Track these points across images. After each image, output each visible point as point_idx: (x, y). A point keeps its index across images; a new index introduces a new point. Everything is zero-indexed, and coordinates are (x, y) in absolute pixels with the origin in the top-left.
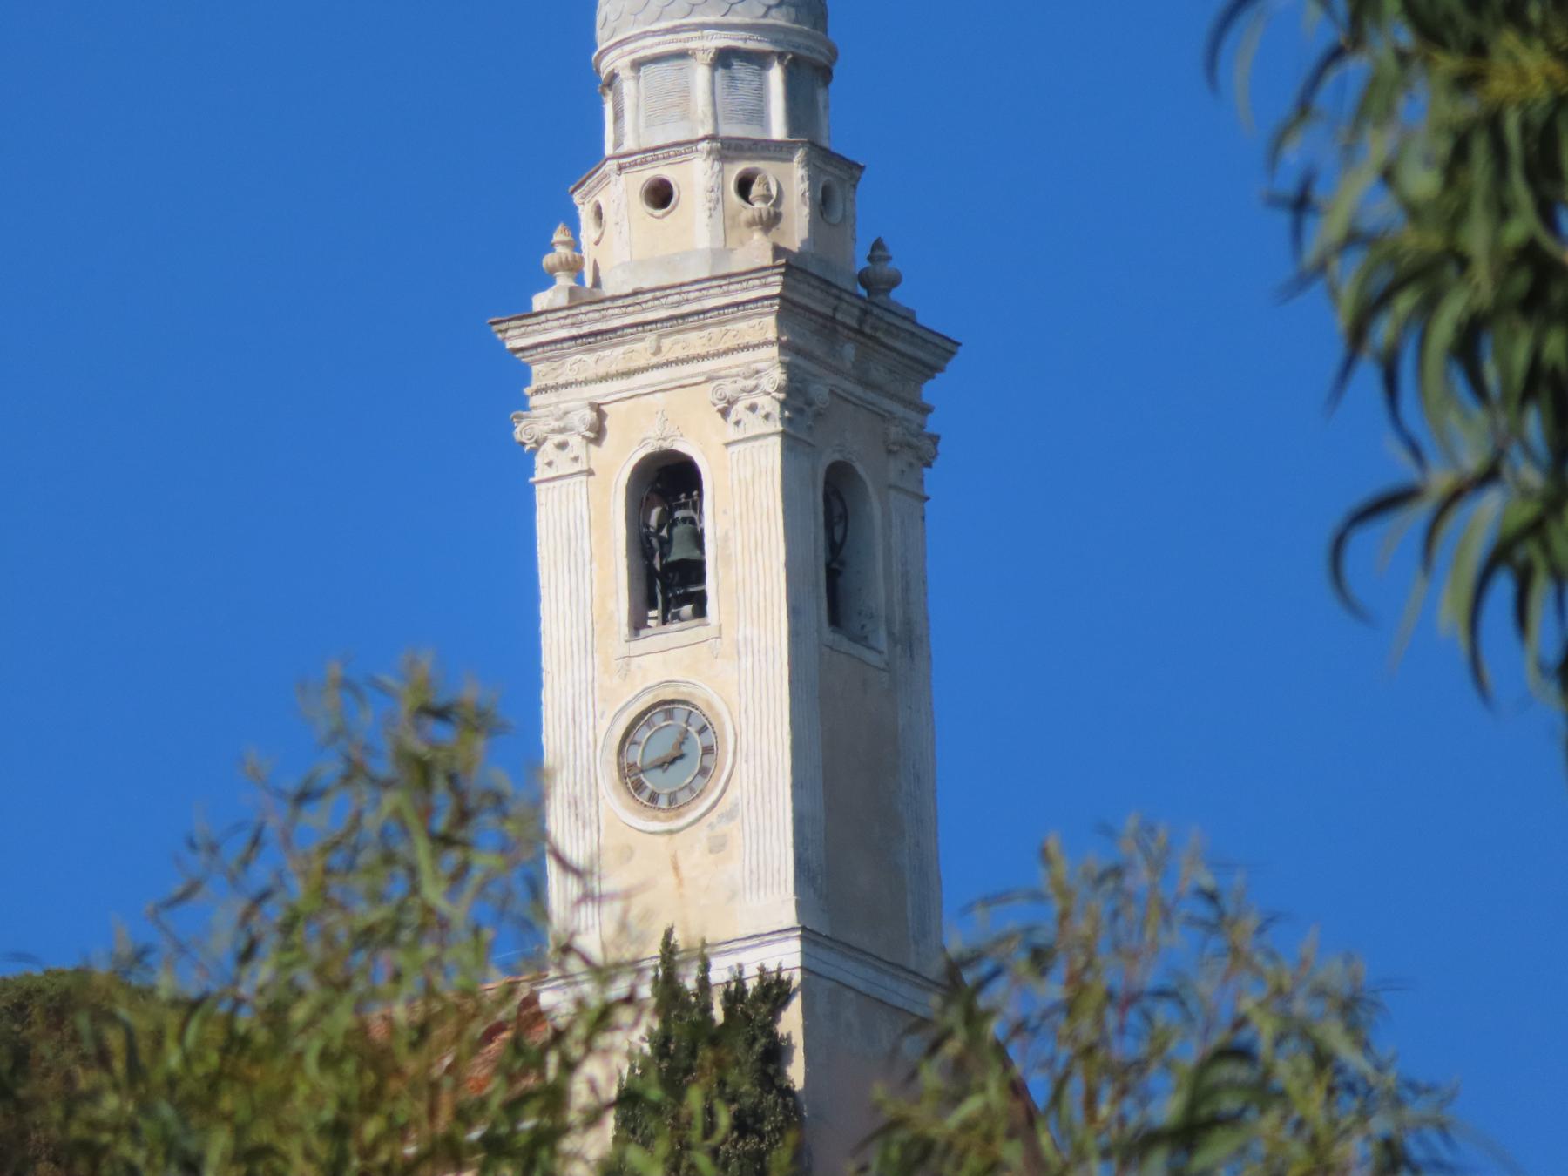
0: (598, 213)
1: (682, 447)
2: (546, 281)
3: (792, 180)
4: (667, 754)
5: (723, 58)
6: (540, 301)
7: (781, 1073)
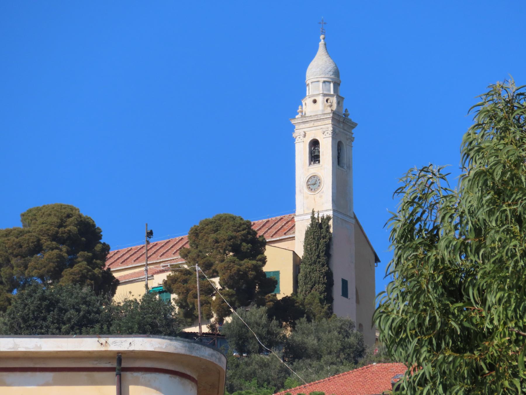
0: (306, 104)
1: (317, 138)
2: (298, 114)
3: (334, 100)
4: (314, 183)
5: (324, 82)
6: (297, 117)
7: (329, 230)
